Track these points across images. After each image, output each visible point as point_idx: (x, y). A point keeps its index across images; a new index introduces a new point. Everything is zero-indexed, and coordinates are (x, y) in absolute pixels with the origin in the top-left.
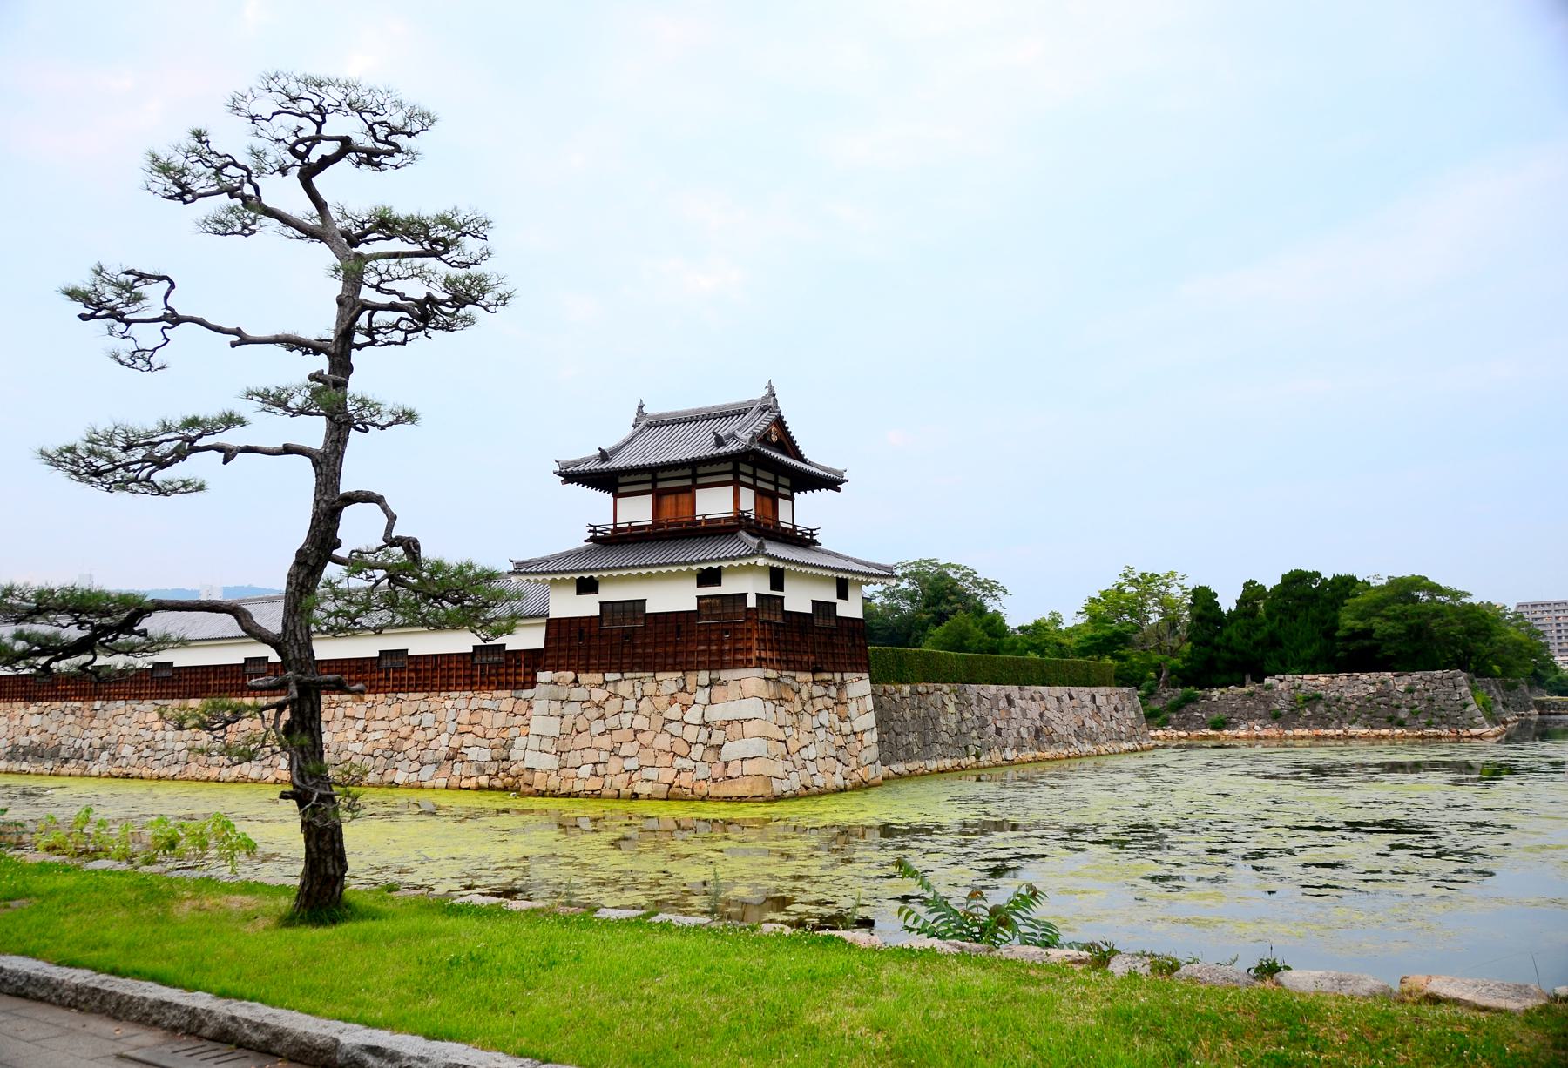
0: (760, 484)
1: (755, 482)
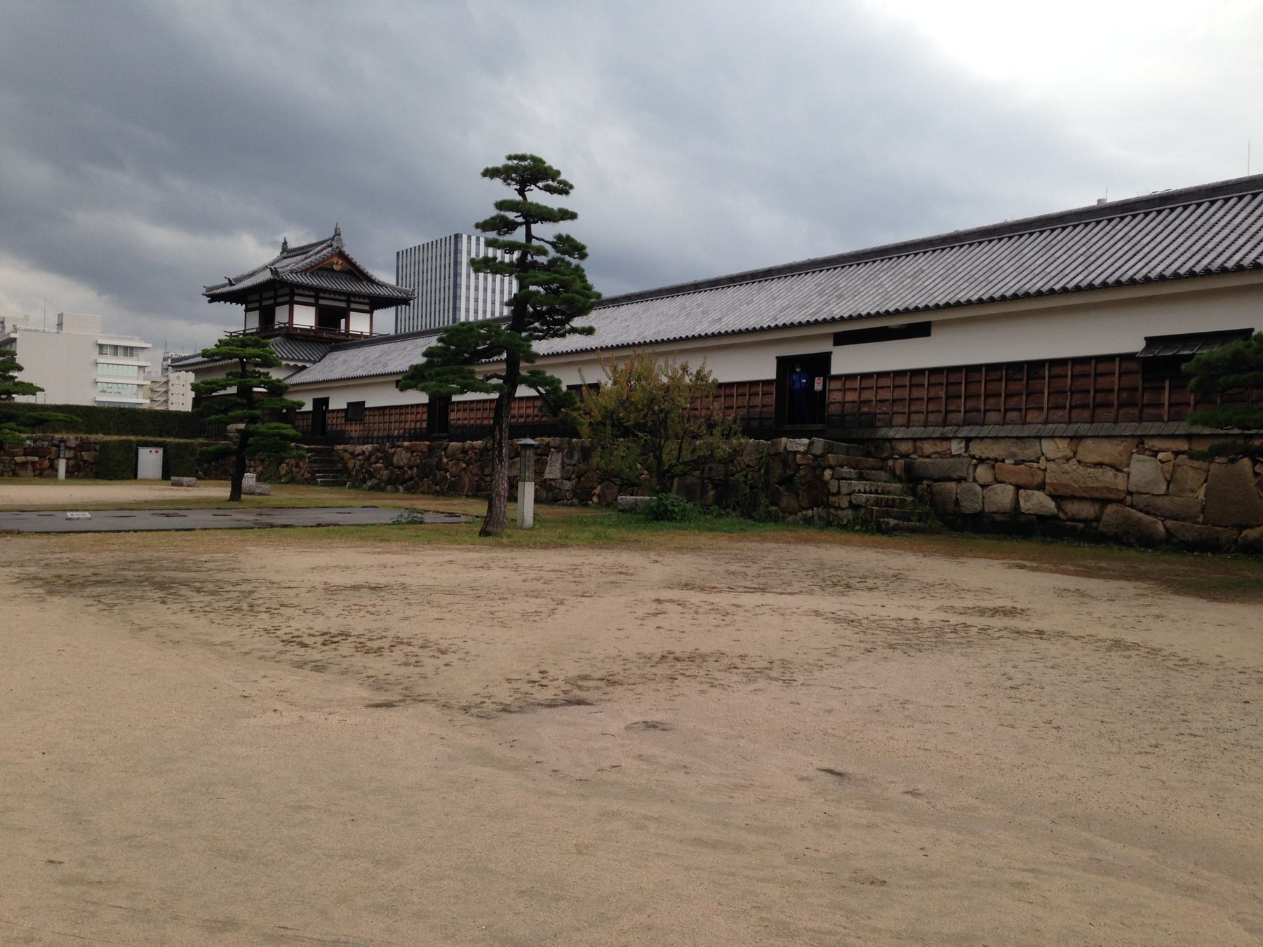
0: (322, 302)
1: (317, 301)
